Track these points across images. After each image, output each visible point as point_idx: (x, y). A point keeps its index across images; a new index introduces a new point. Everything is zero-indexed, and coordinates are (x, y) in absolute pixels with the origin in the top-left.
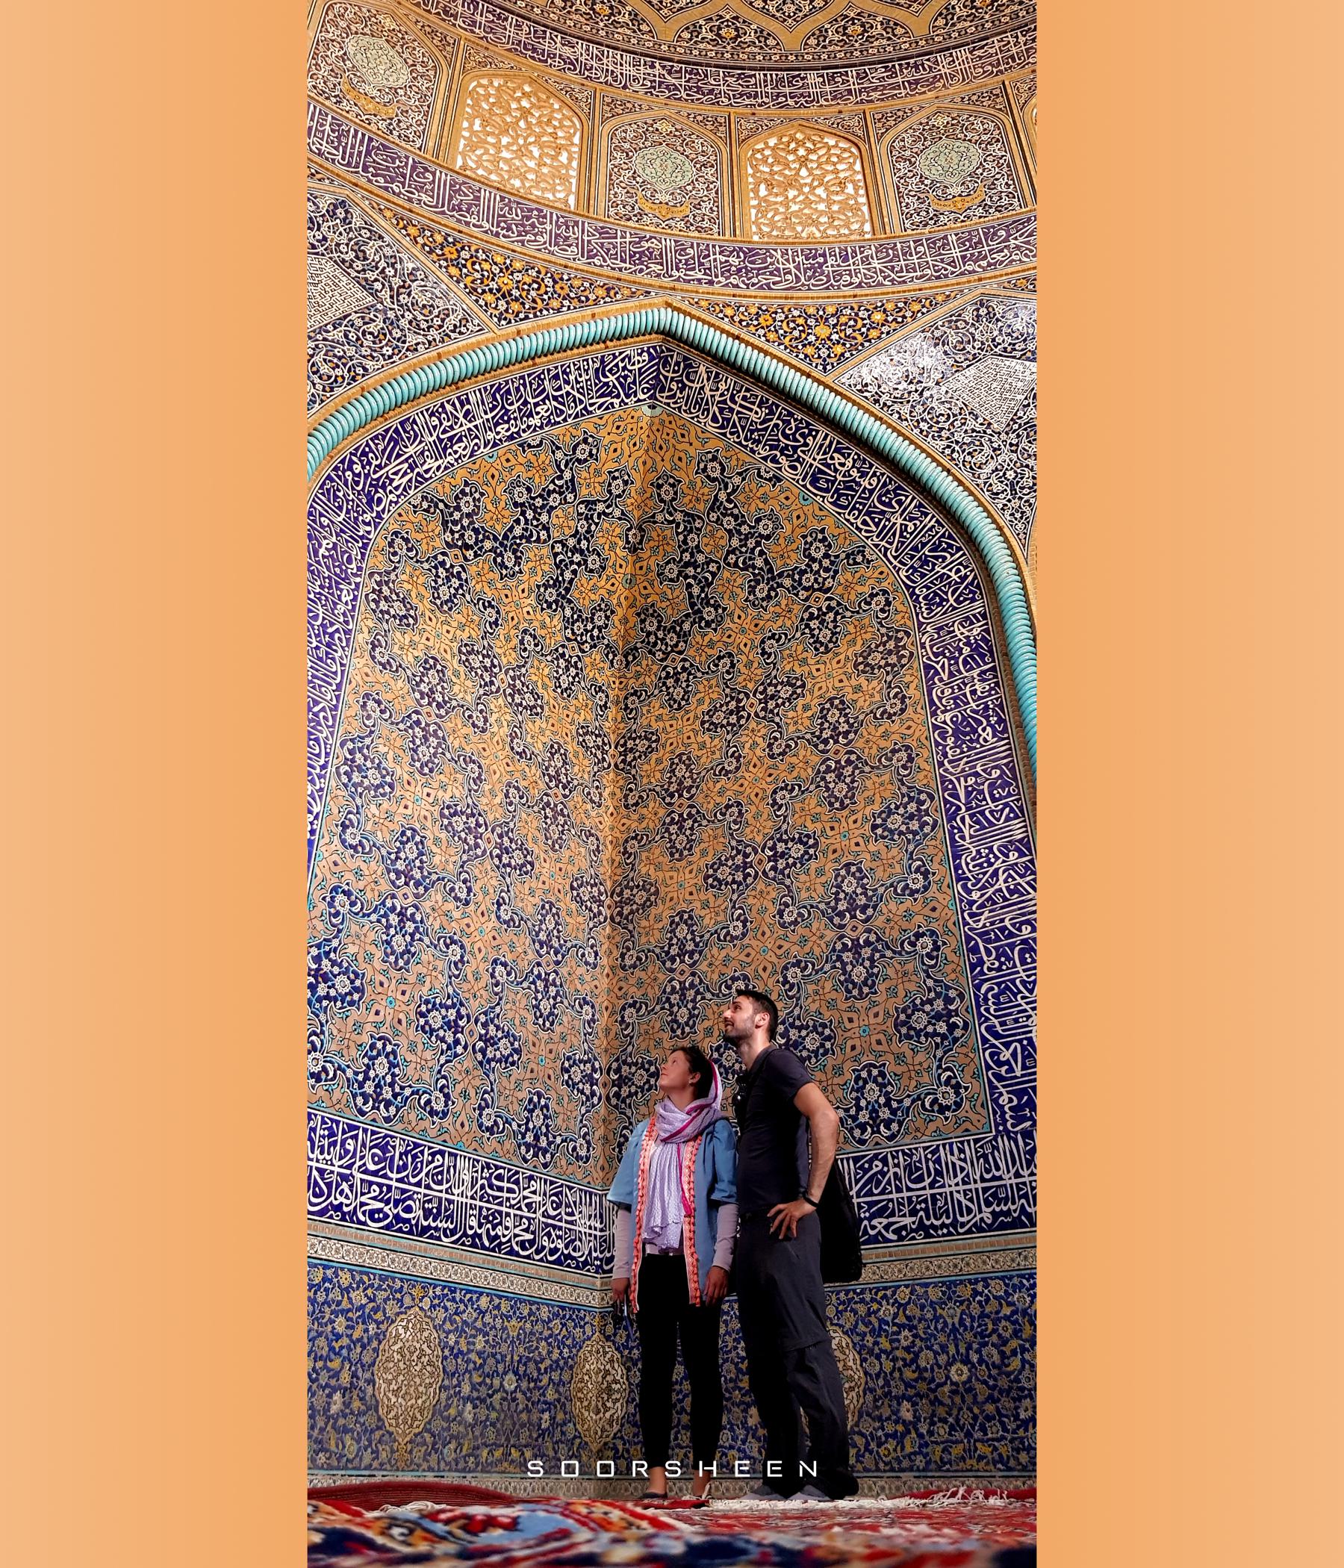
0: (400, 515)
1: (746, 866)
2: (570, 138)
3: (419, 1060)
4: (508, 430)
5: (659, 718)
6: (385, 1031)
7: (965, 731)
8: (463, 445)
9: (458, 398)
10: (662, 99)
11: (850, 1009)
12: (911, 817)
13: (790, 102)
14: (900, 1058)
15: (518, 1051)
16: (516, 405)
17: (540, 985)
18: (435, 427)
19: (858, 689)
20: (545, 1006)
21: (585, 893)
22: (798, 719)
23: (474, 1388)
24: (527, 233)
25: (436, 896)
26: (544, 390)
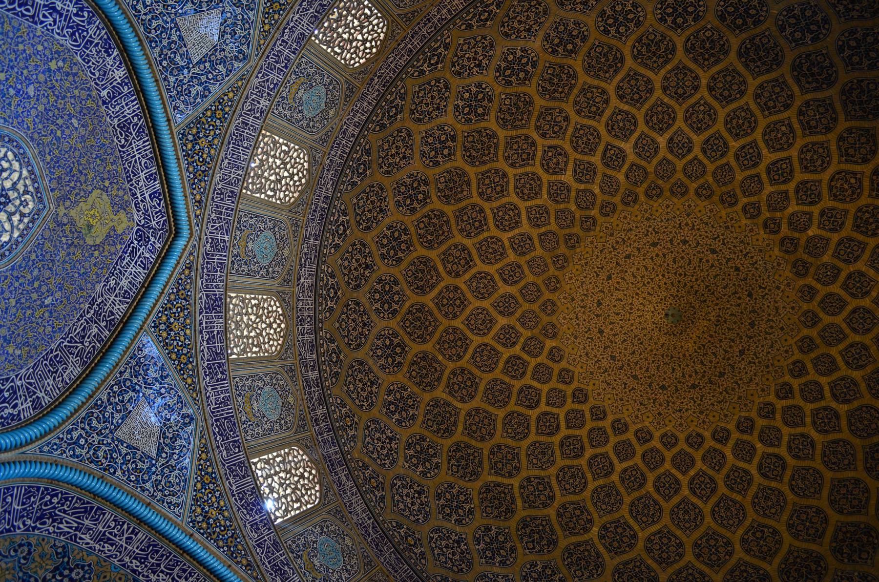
0: (43, 540)
2: (308, 503)
4: (137, 566)
8: (110, 548)
9: (134, 528)
10: (359, 532)
16: (153, 561)
18: (109, 526)
26: (173, 570)
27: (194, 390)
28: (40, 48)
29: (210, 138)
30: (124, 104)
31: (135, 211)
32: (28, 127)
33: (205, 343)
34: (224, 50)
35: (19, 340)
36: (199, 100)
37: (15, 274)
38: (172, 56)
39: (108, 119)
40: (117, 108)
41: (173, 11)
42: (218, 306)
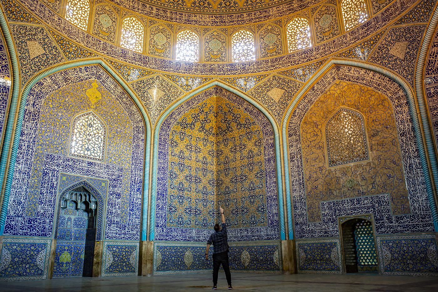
1: (237, 179)
3: (186, 217)
5: (223, 148)
6: (180, 214)
7: (269, 160)
11: (251, 206)
12: (261, 175)
13: (240, 23)
14: (257, 214)
15: (201, 212)
17: (204, 201)
19: (254, 149)
20: (205, 204)
21: (211, 183)
22: (245, 153)
23: (198, 259)
24: (190, 70)
25: (186, 192)
27: (150, 72)
28: (47, 110)
29: (70, 46)
30: (58, 79)
31: (91, 79)
32: (71, 116)
33: (136, 62)
34: (40, 39)
35: (125, 124)
36: (57, 51)
37: (109, 124)
38: (43, 61)
39: (64, 86)
40: (60, 82)
41: (29, 61)
42: (125, 52)
